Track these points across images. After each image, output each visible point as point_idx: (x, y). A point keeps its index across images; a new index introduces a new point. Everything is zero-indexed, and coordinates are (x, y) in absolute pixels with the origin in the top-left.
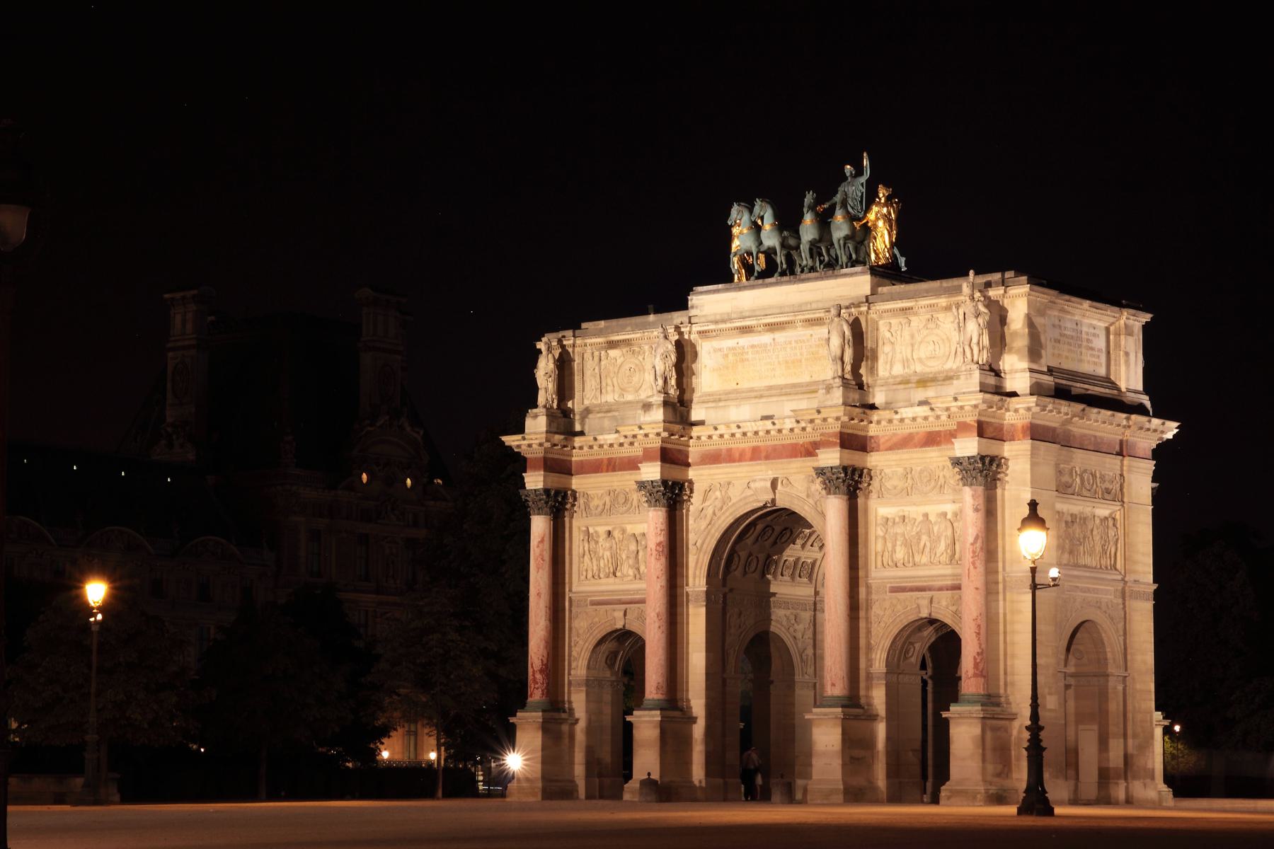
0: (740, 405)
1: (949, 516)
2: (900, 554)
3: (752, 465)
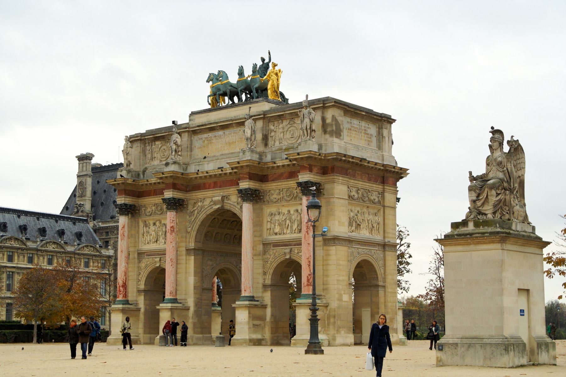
1: (299, 211)
2: (277, 230)
3: (214, 190)
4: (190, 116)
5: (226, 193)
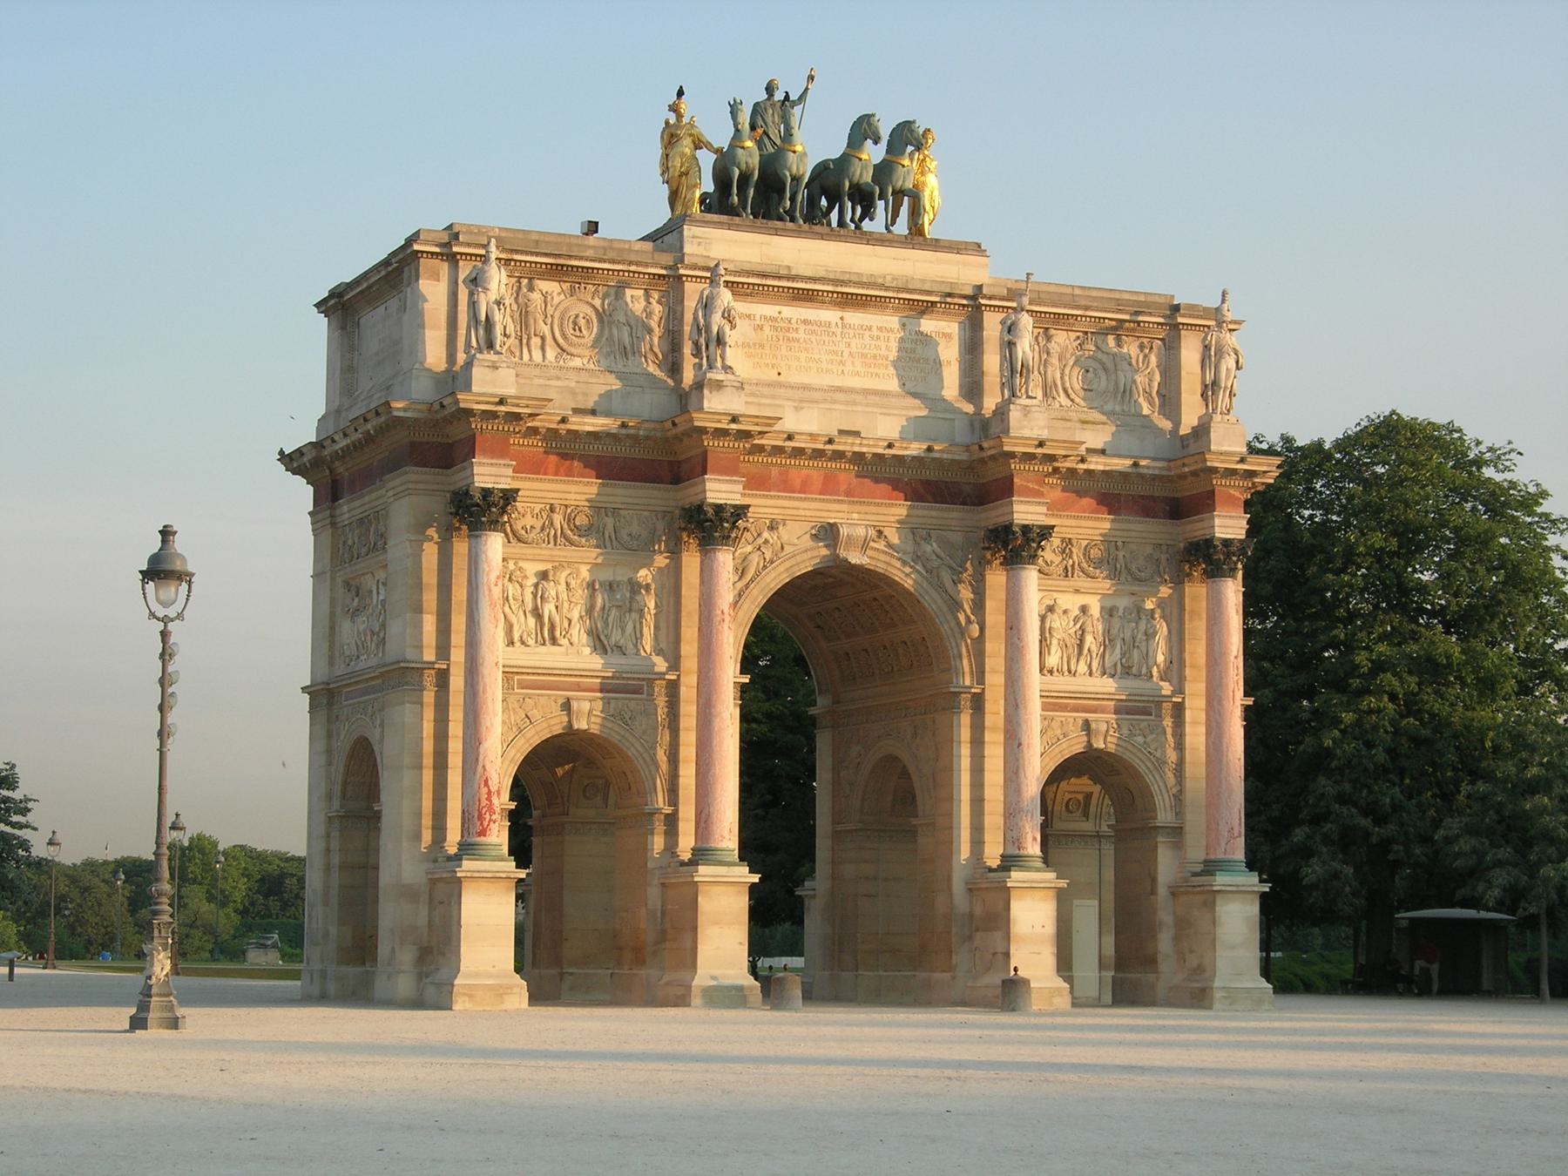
0: (802, 408)
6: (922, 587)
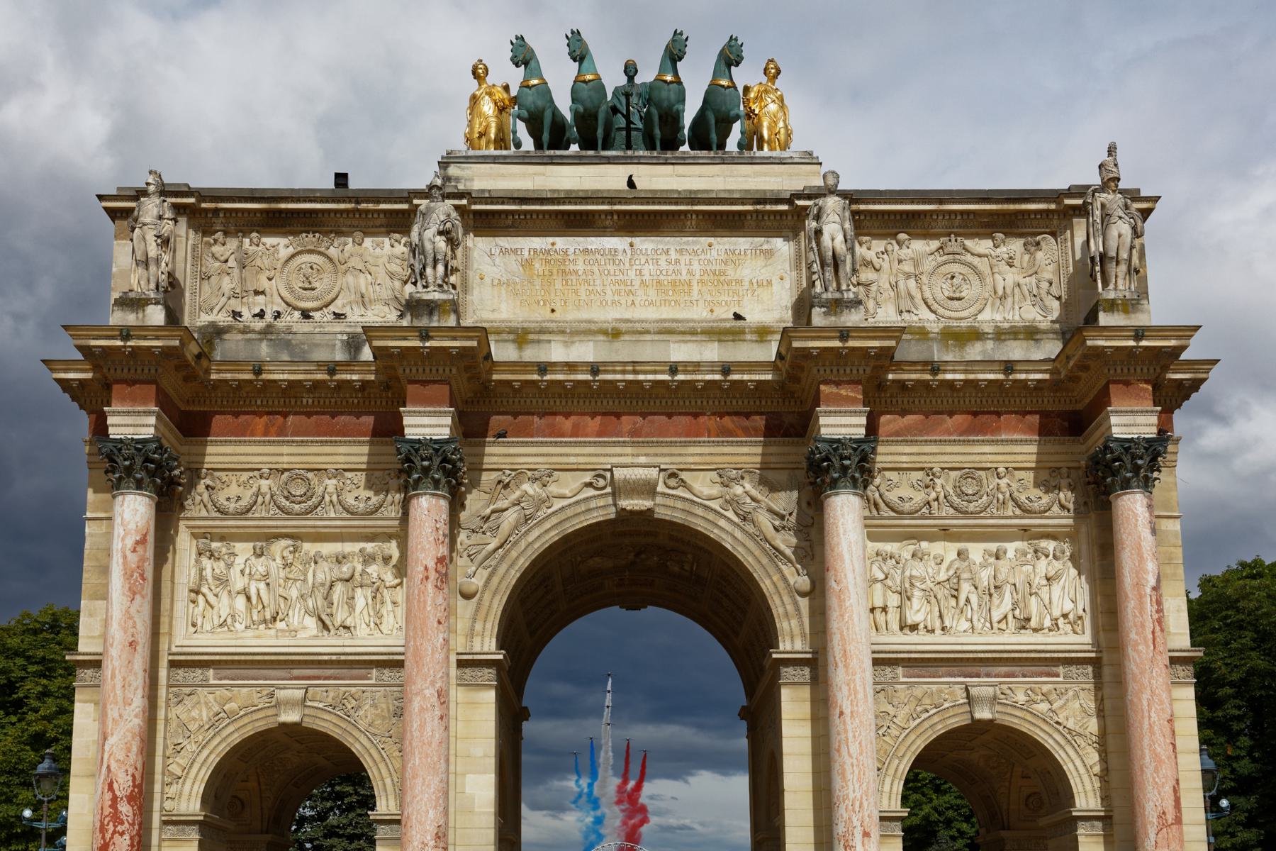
0: (573, 342)
1: (1011, 554)
2: (917, 612)
4: (444, 164)
5: (667, 460)
6: (733, 536)
